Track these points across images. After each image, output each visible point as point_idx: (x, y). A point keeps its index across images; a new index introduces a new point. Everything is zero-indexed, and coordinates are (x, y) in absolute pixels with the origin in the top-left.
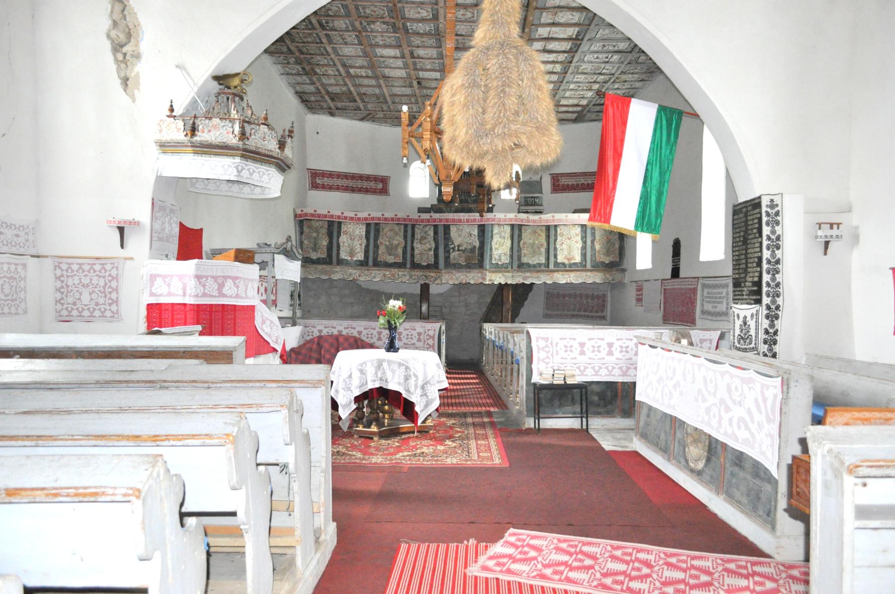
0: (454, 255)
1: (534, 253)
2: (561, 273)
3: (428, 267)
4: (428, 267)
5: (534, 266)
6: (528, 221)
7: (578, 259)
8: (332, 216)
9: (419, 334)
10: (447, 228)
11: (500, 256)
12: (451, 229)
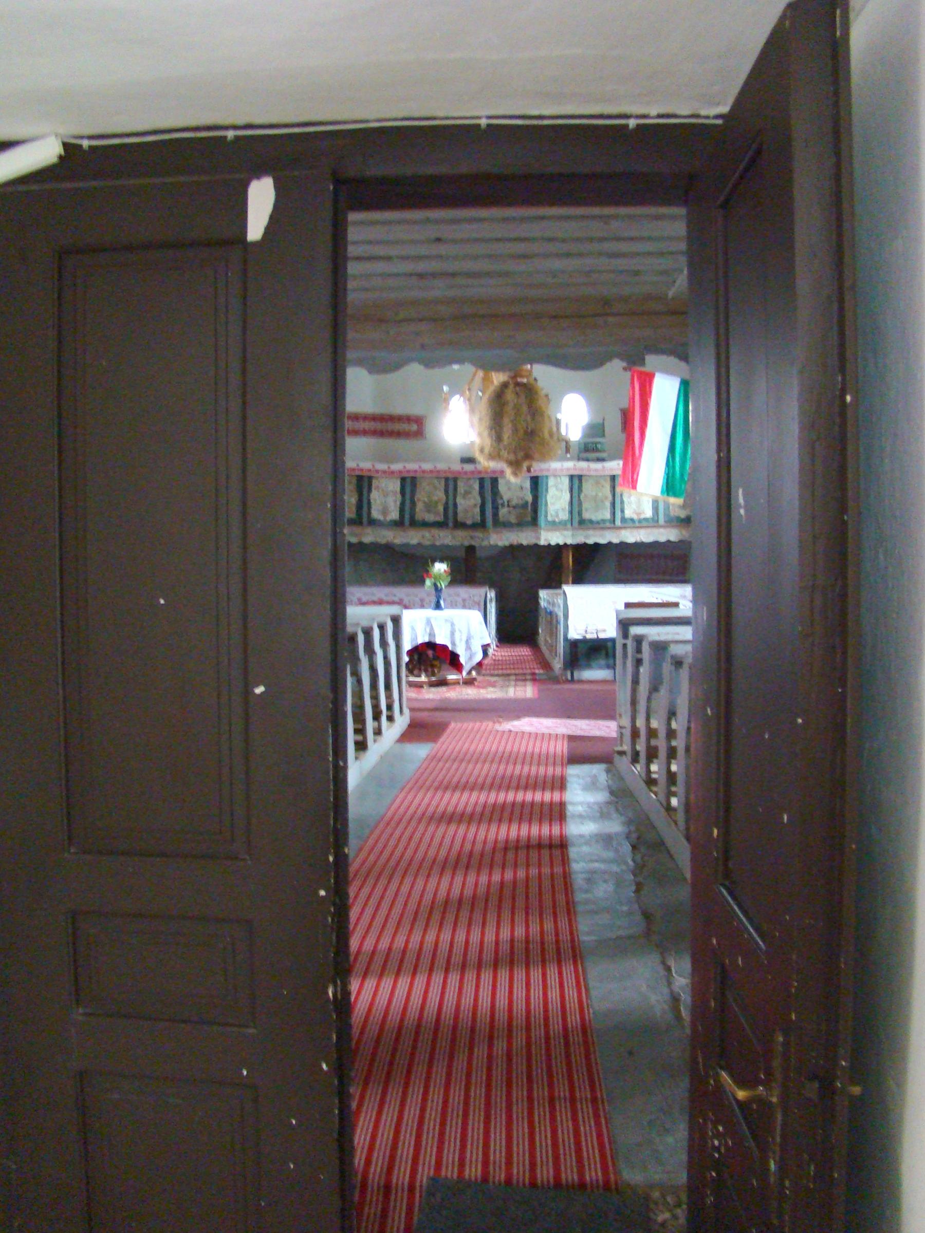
0: (503, 512)
1: (597, 509)
3: (475, 526)
4: (475, 526)
5: (598, 523)
6: (589, 469)
7: (648, 513)
8: (362, 470)
9: (464, 600)
11: (557, 513)
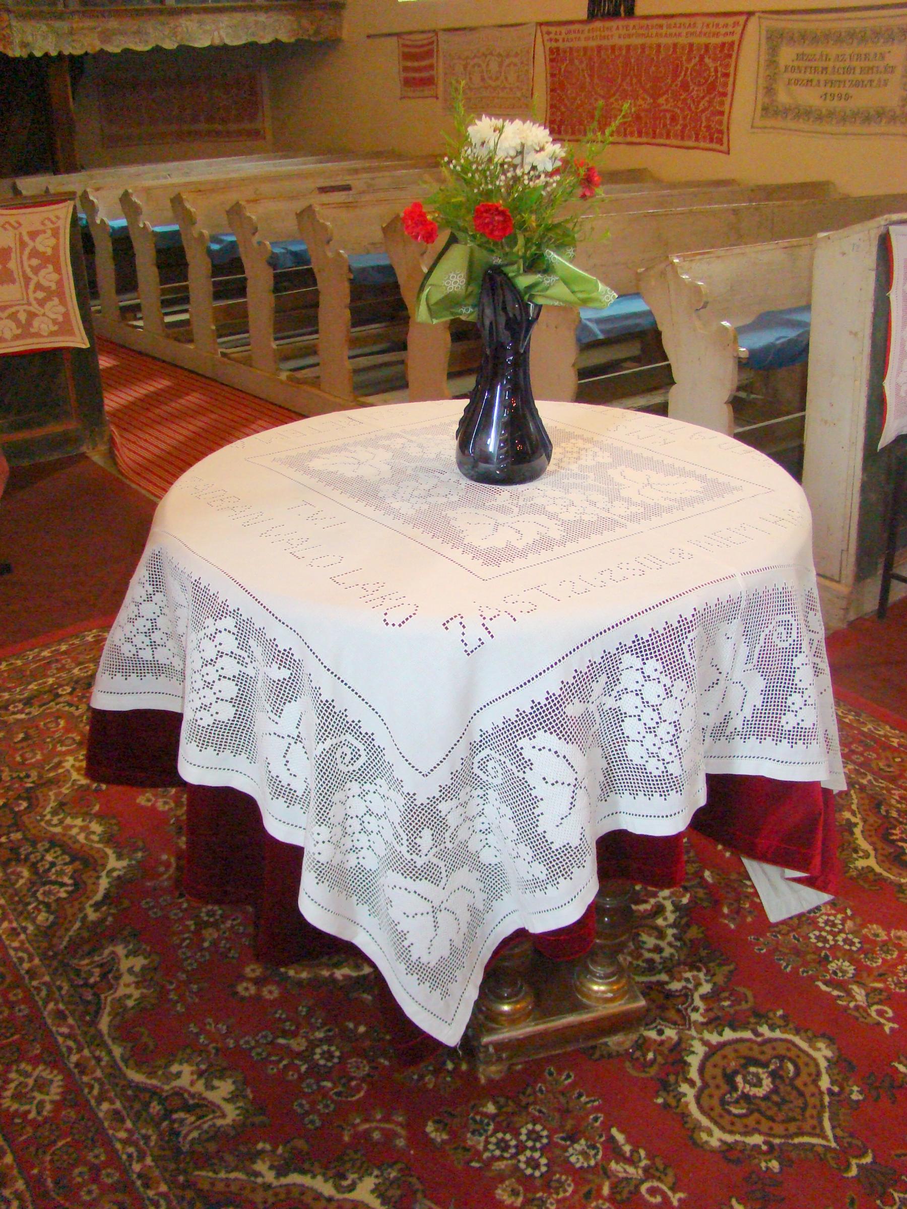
2: (195, 17)
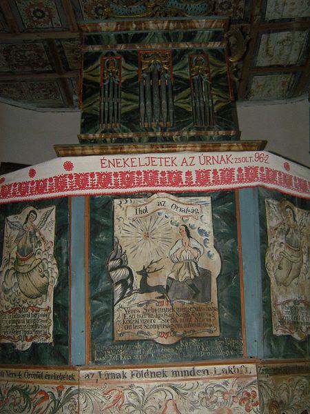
0: (128, 306)
10: (101, 211)
12: (118, 211)
